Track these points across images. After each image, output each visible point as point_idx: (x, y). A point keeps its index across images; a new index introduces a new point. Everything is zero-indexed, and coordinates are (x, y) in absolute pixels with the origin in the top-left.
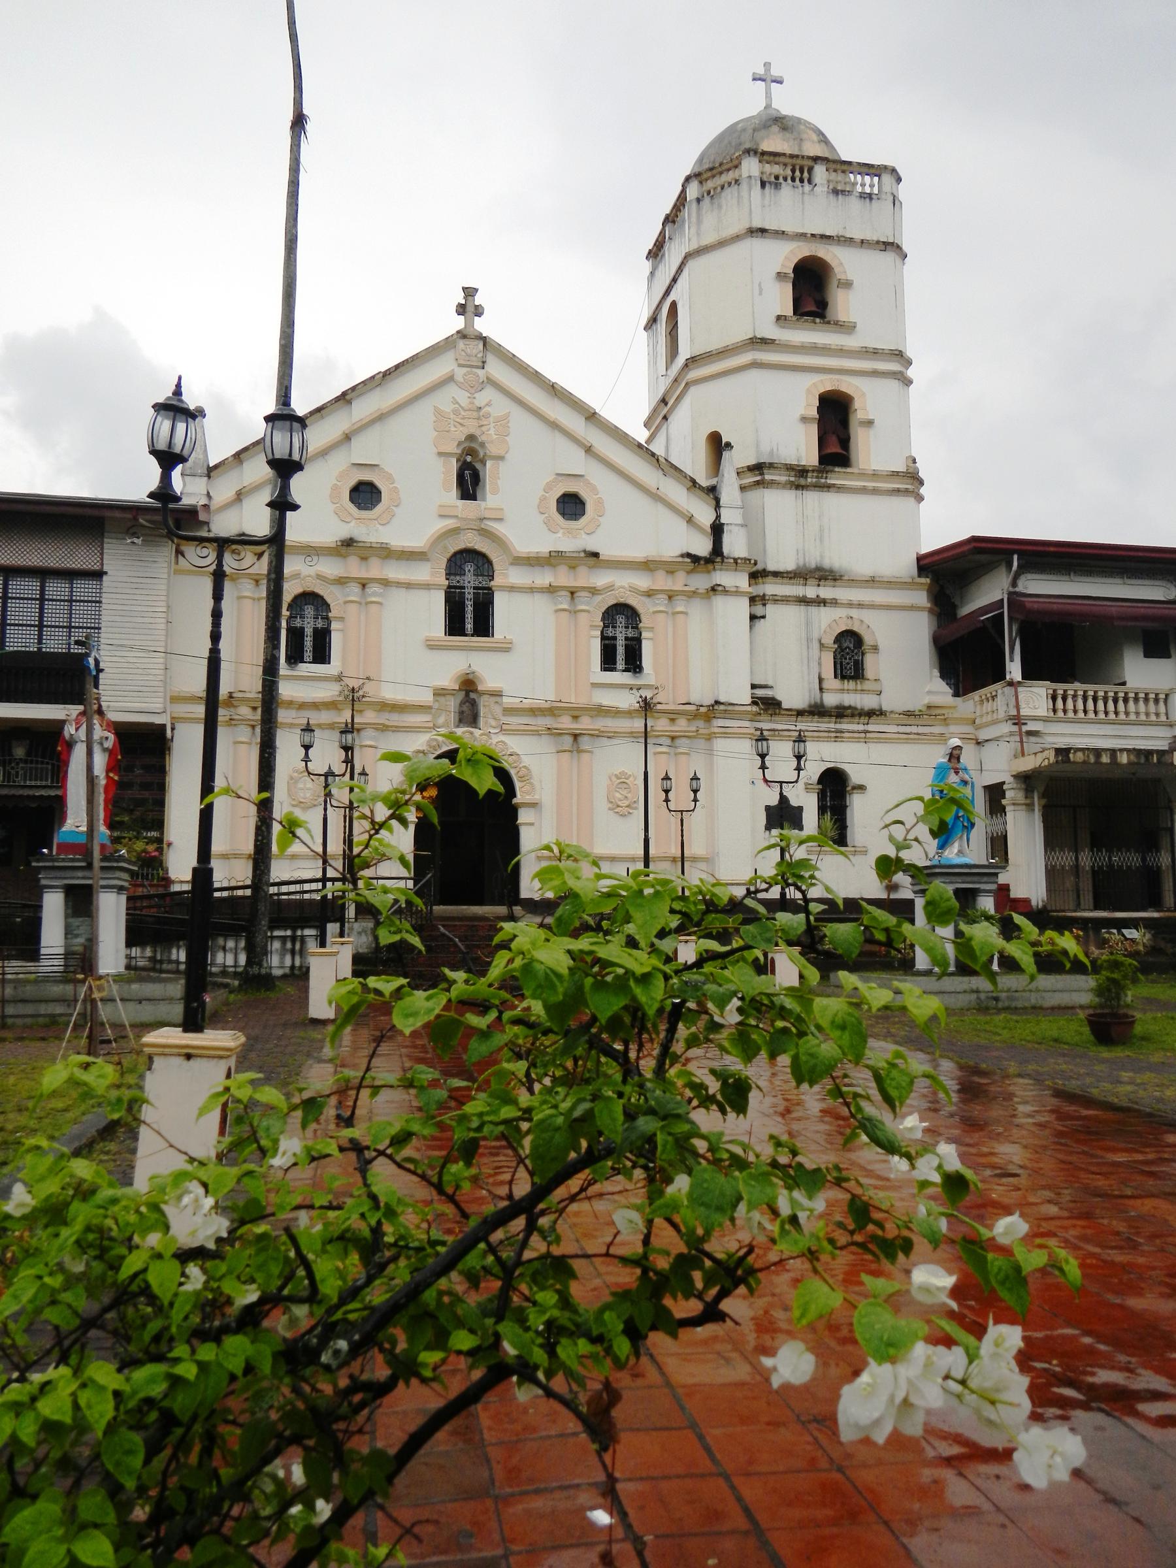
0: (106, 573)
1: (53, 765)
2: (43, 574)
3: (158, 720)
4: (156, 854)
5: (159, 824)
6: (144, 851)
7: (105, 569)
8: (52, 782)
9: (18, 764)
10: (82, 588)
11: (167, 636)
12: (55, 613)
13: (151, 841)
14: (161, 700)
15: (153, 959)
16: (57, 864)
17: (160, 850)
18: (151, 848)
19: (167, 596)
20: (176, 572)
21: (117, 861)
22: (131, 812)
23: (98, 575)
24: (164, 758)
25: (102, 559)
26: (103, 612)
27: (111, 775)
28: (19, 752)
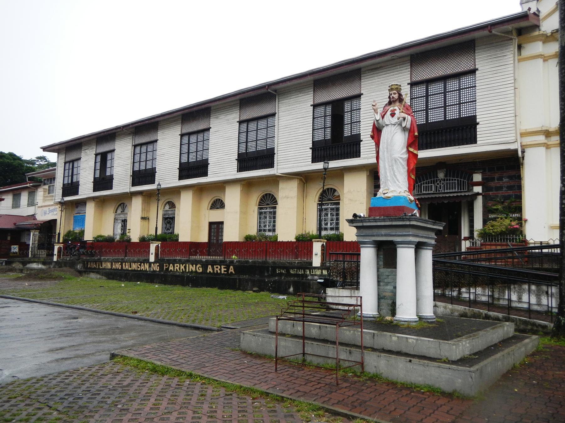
0: (477, 69)
1: (458, 180)
2: (444, 79)
3: (512, 147)
4: (517, 226)
5: (519, 209)
6: (510, 225)
7: (477, 67)
8: (458, 189)
9: (440, 182)
10: (466, 81)
11: (515, 96)
12: (452, 99)
13: (514, 219)
14: (514, 135)
15: (492, 296)
16: (365, 224)
17: (521, 225)
18: (514, 223)
19: (514, 73)
20: (519, 61)
21: (409, 220)
22: (503, 203)
23: (473, 72)
24: (520, 171)
25: (475, 63)
26: (477, 91)
27: (411, 150)
28: (441, 175)
